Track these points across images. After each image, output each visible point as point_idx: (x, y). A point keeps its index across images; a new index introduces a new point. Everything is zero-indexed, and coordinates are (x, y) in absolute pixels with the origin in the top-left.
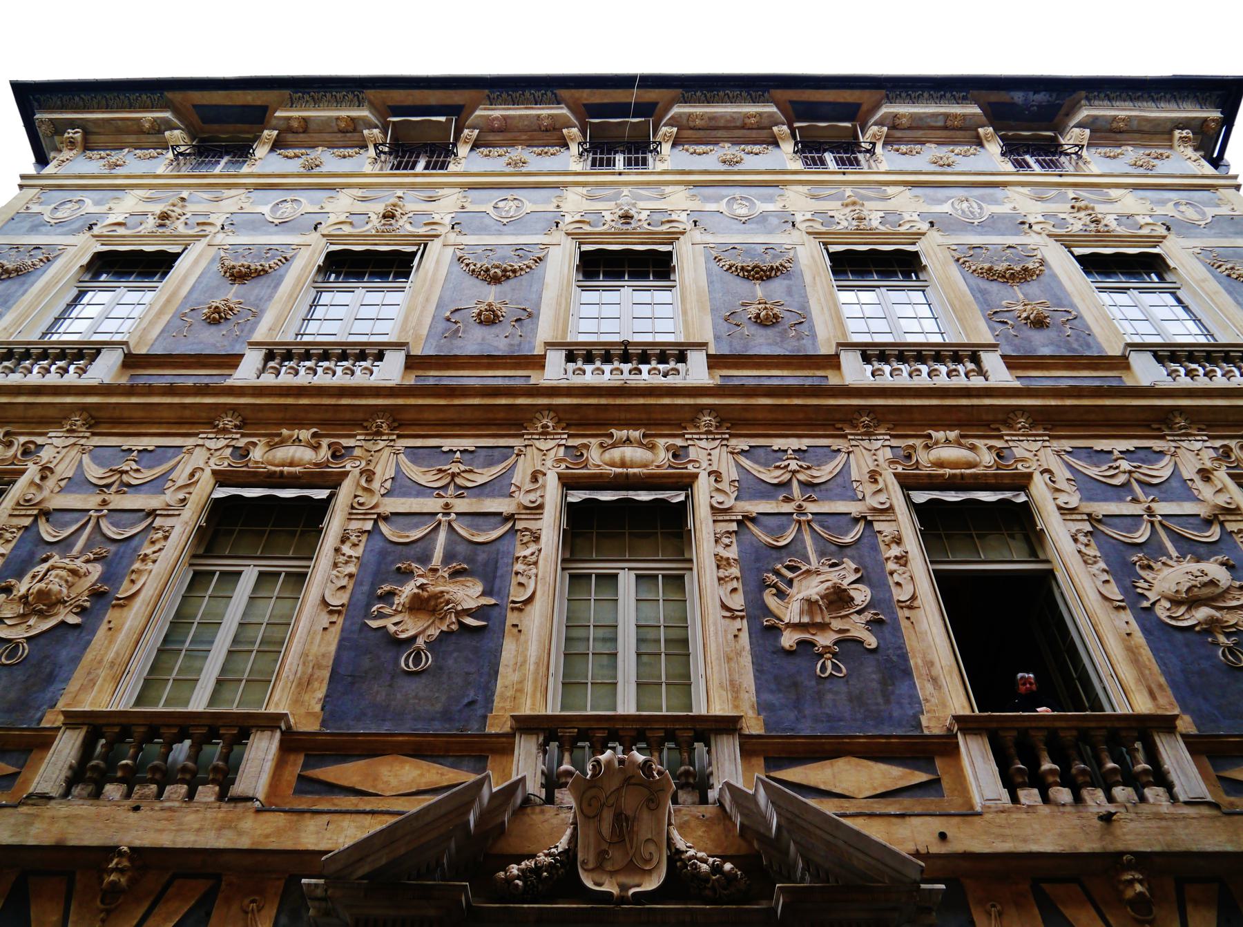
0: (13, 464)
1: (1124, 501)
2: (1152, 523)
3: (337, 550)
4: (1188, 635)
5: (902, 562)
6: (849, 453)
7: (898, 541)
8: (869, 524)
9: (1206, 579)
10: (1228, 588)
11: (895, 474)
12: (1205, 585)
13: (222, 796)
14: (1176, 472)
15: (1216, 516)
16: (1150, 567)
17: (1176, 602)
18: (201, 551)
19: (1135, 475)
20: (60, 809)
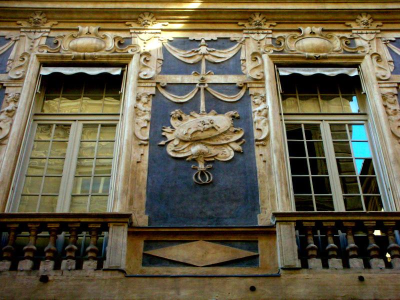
1: (190, 74)
2: (199, 89)
4: (180, 163)
5: (11, 114)
6: (15, 41)
7: (16, 100)
8: (5, 87)
9: (211, 125)
10: (225, 132)
11: (38, 56)
12: (208, 129)
14: (237, 56)
15: (245, 84)
16: (180, 118)
17: (184, 141)
19: (206, 57)
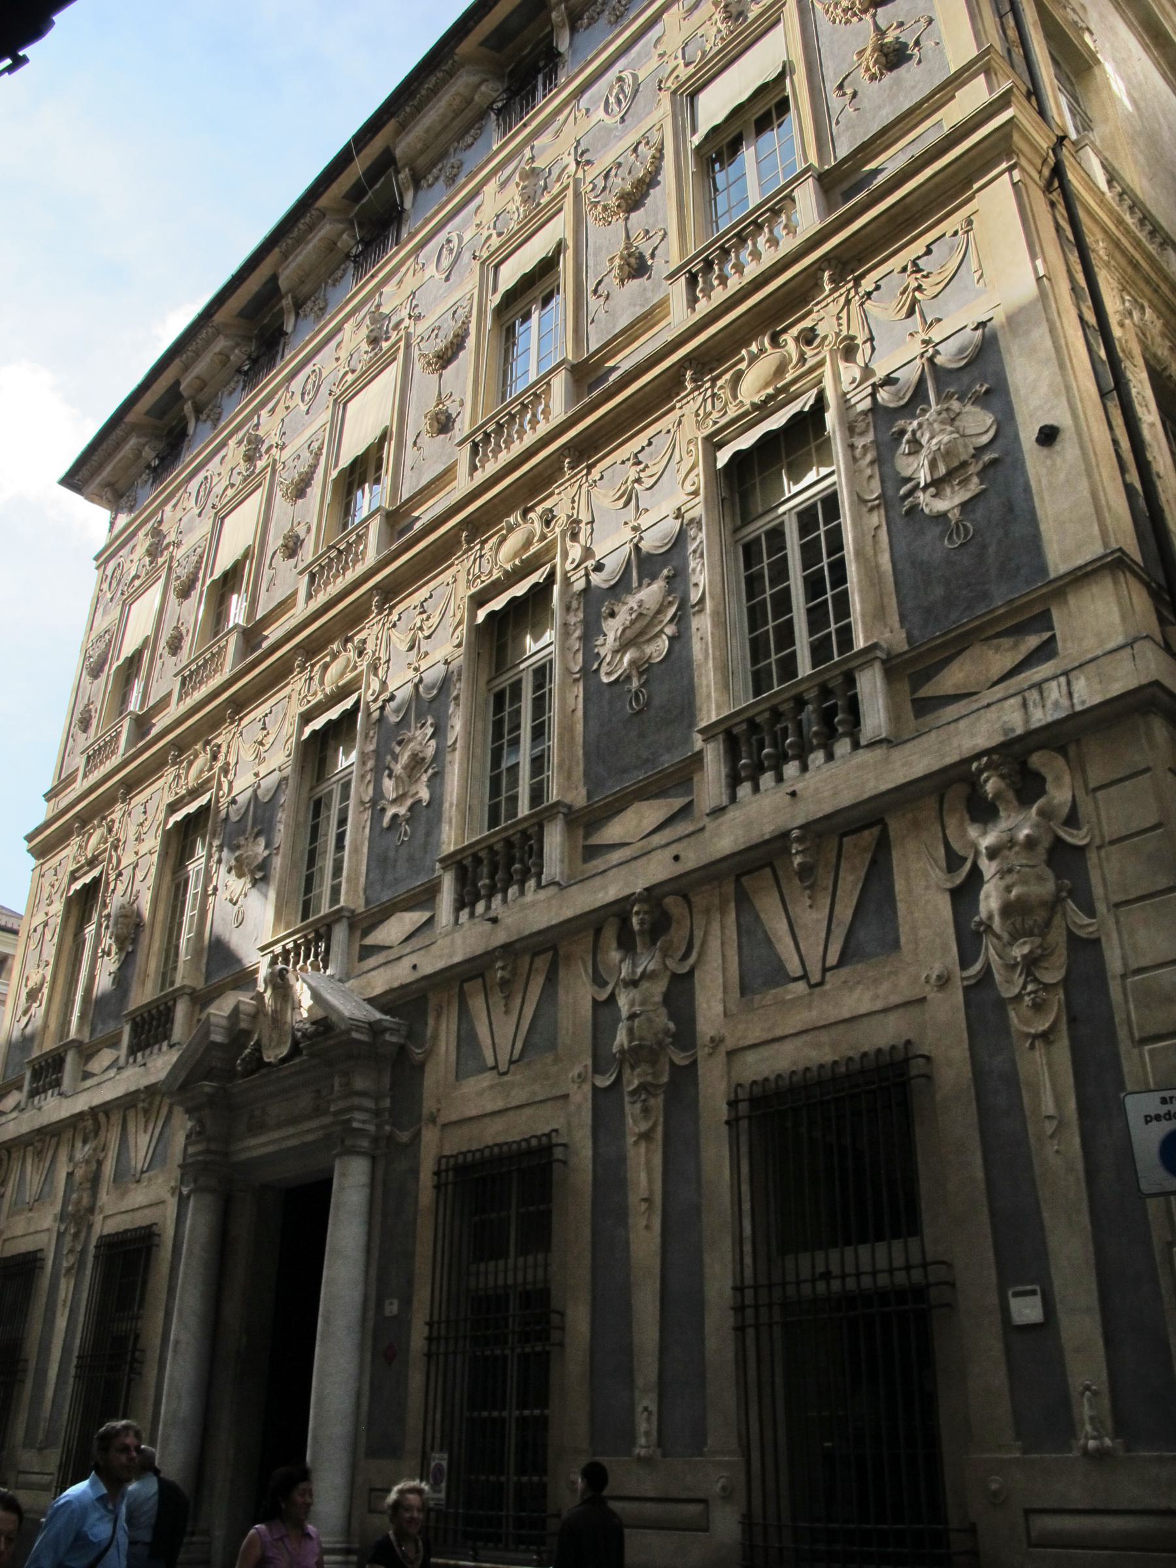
0: (546, 538)
3: (852, 447)
13: (856, 745)
18: (739, 522)
20: (734, 815)
